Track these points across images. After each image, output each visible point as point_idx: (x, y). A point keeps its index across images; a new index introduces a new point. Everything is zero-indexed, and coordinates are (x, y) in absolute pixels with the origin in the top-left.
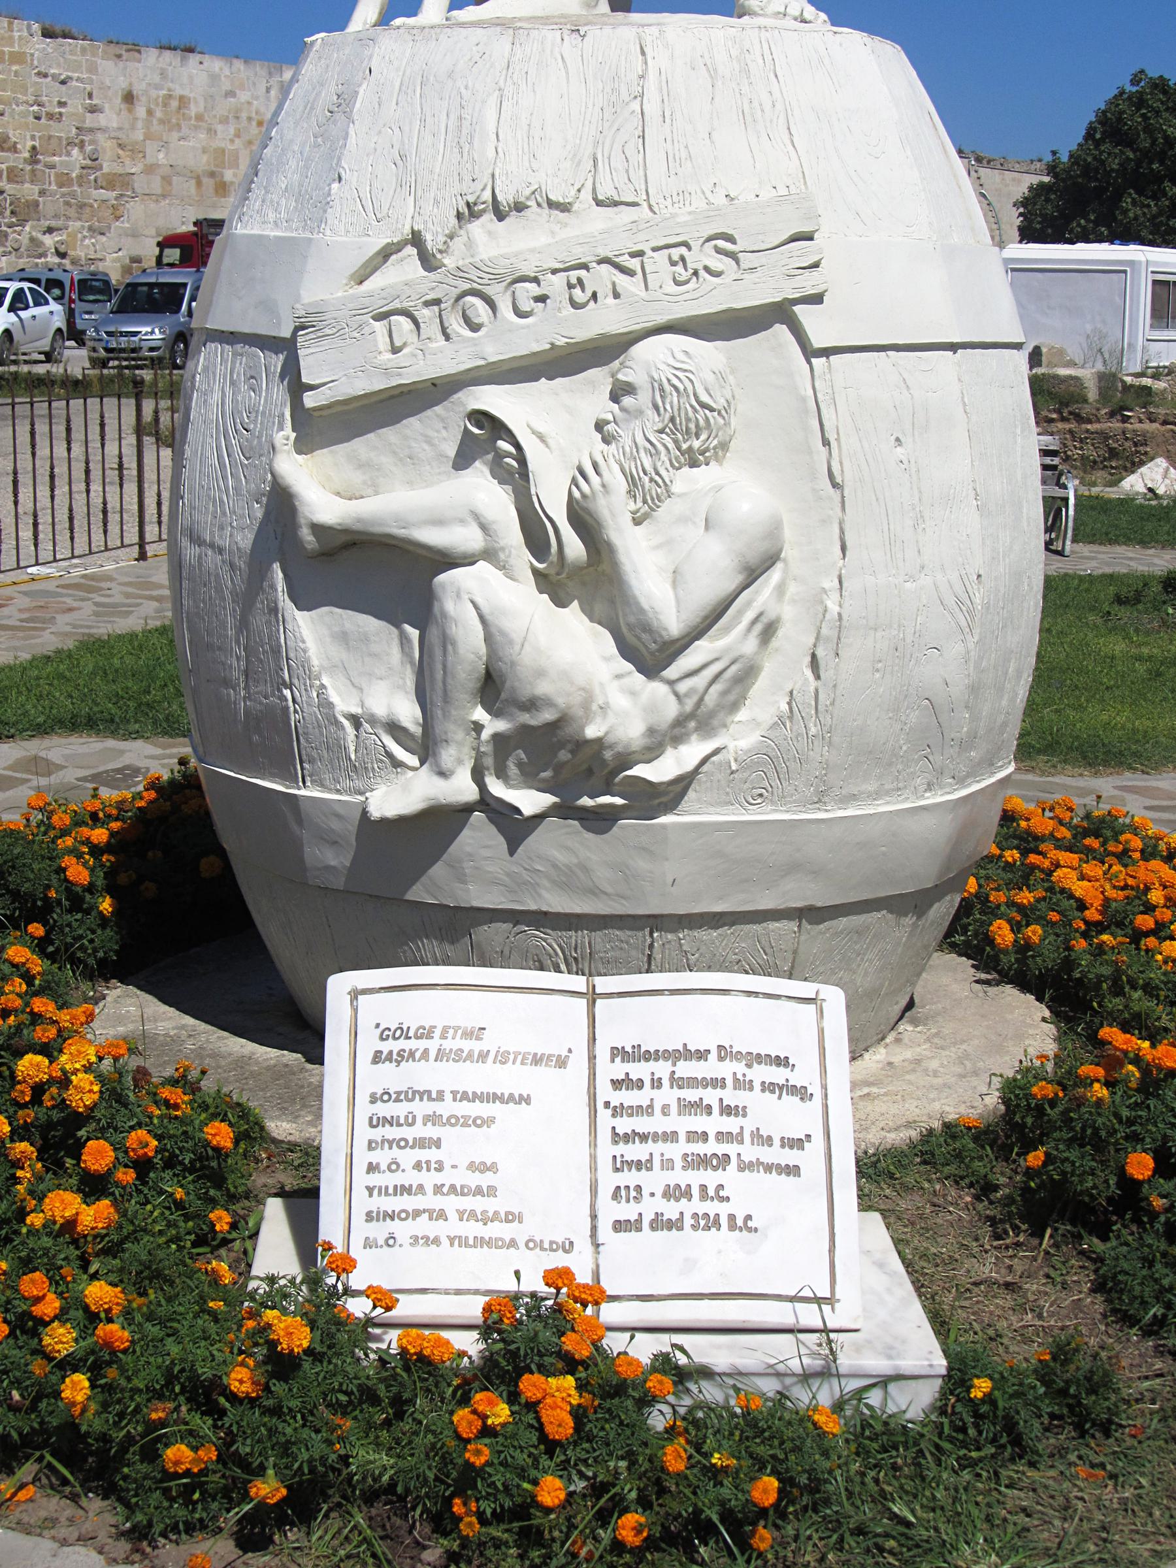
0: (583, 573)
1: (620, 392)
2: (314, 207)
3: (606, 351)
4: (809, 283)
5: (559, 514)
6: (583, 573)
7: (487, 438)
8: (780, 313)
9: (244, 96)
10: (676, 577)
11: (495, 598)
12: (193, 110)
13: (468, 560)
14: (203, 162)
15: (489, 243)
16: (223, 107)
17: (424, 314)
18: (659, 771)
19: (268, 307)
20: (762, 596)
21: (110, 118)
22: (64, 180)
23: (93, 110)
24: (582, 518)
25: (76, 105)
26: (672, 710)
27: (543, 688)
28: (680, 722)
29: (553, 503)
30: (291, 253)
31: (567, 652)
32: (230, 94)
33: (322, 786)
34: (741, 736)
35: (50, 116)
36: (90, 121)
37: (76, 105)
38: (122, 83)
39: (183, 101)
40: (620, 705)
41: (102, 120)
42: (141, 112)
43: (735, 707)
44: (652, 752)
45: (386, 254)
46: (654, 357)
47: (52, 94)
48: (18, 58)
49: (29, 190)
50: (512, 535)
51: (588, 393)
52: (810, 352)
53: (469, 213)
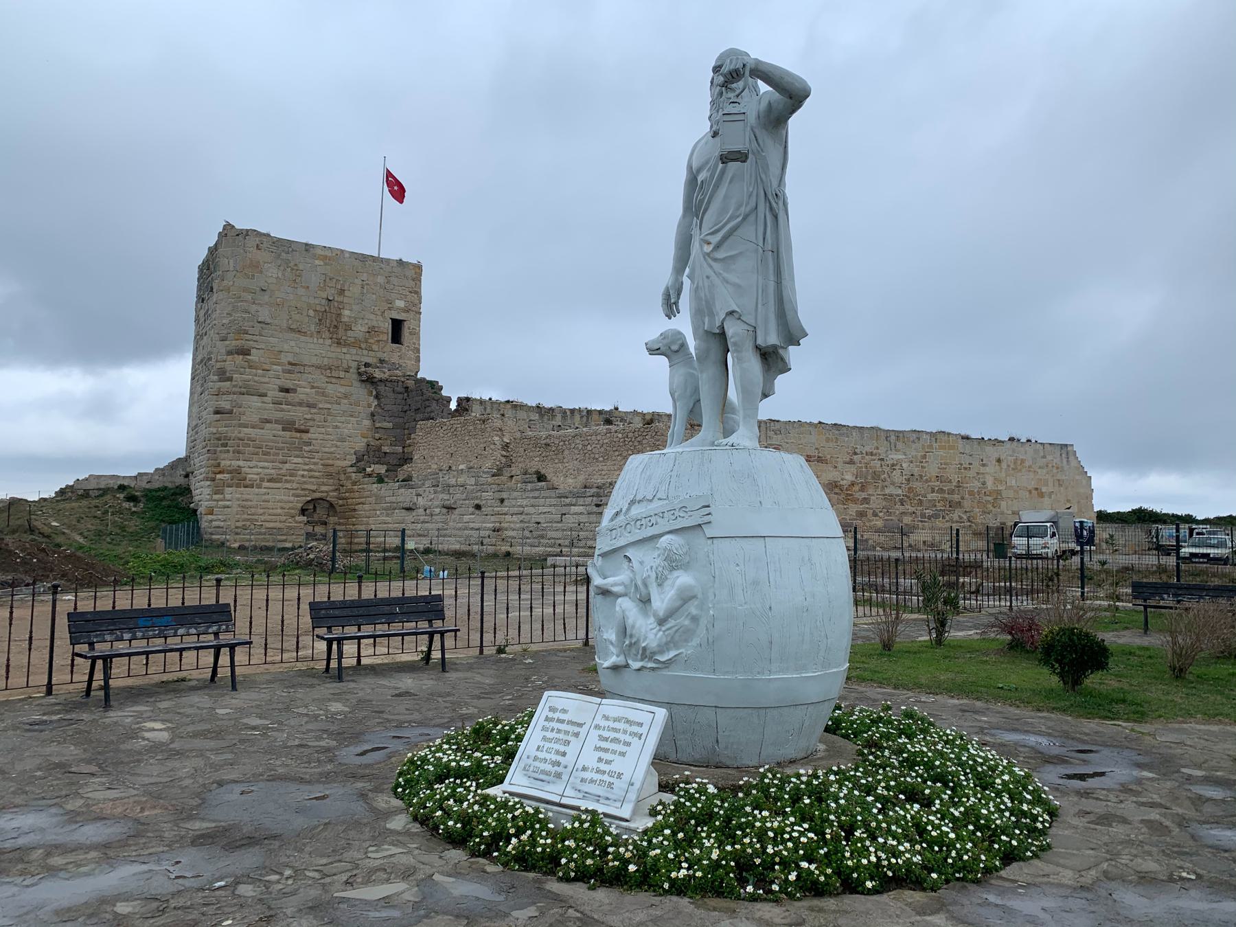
4: (706, 519)
9: (1049, 458)
12: (1027, 464)
14: (1033, 485)
15: (636, 511)
16: (1042, 462)
20: (693, 609)
21: (991, 469)
22: (971, 493)
23: (984, 465)
25: (976, 464)
28: (667, 644)
32: (1044, 457)
36: (982, 470)
37: (976, 464)
38: (996, 455)
39: (1023, 461)
41: (987, 469)
42: (1004, 465)
44: (661, 652)
47: (966, 460)
49: (956, 497)
53: (632, 502)
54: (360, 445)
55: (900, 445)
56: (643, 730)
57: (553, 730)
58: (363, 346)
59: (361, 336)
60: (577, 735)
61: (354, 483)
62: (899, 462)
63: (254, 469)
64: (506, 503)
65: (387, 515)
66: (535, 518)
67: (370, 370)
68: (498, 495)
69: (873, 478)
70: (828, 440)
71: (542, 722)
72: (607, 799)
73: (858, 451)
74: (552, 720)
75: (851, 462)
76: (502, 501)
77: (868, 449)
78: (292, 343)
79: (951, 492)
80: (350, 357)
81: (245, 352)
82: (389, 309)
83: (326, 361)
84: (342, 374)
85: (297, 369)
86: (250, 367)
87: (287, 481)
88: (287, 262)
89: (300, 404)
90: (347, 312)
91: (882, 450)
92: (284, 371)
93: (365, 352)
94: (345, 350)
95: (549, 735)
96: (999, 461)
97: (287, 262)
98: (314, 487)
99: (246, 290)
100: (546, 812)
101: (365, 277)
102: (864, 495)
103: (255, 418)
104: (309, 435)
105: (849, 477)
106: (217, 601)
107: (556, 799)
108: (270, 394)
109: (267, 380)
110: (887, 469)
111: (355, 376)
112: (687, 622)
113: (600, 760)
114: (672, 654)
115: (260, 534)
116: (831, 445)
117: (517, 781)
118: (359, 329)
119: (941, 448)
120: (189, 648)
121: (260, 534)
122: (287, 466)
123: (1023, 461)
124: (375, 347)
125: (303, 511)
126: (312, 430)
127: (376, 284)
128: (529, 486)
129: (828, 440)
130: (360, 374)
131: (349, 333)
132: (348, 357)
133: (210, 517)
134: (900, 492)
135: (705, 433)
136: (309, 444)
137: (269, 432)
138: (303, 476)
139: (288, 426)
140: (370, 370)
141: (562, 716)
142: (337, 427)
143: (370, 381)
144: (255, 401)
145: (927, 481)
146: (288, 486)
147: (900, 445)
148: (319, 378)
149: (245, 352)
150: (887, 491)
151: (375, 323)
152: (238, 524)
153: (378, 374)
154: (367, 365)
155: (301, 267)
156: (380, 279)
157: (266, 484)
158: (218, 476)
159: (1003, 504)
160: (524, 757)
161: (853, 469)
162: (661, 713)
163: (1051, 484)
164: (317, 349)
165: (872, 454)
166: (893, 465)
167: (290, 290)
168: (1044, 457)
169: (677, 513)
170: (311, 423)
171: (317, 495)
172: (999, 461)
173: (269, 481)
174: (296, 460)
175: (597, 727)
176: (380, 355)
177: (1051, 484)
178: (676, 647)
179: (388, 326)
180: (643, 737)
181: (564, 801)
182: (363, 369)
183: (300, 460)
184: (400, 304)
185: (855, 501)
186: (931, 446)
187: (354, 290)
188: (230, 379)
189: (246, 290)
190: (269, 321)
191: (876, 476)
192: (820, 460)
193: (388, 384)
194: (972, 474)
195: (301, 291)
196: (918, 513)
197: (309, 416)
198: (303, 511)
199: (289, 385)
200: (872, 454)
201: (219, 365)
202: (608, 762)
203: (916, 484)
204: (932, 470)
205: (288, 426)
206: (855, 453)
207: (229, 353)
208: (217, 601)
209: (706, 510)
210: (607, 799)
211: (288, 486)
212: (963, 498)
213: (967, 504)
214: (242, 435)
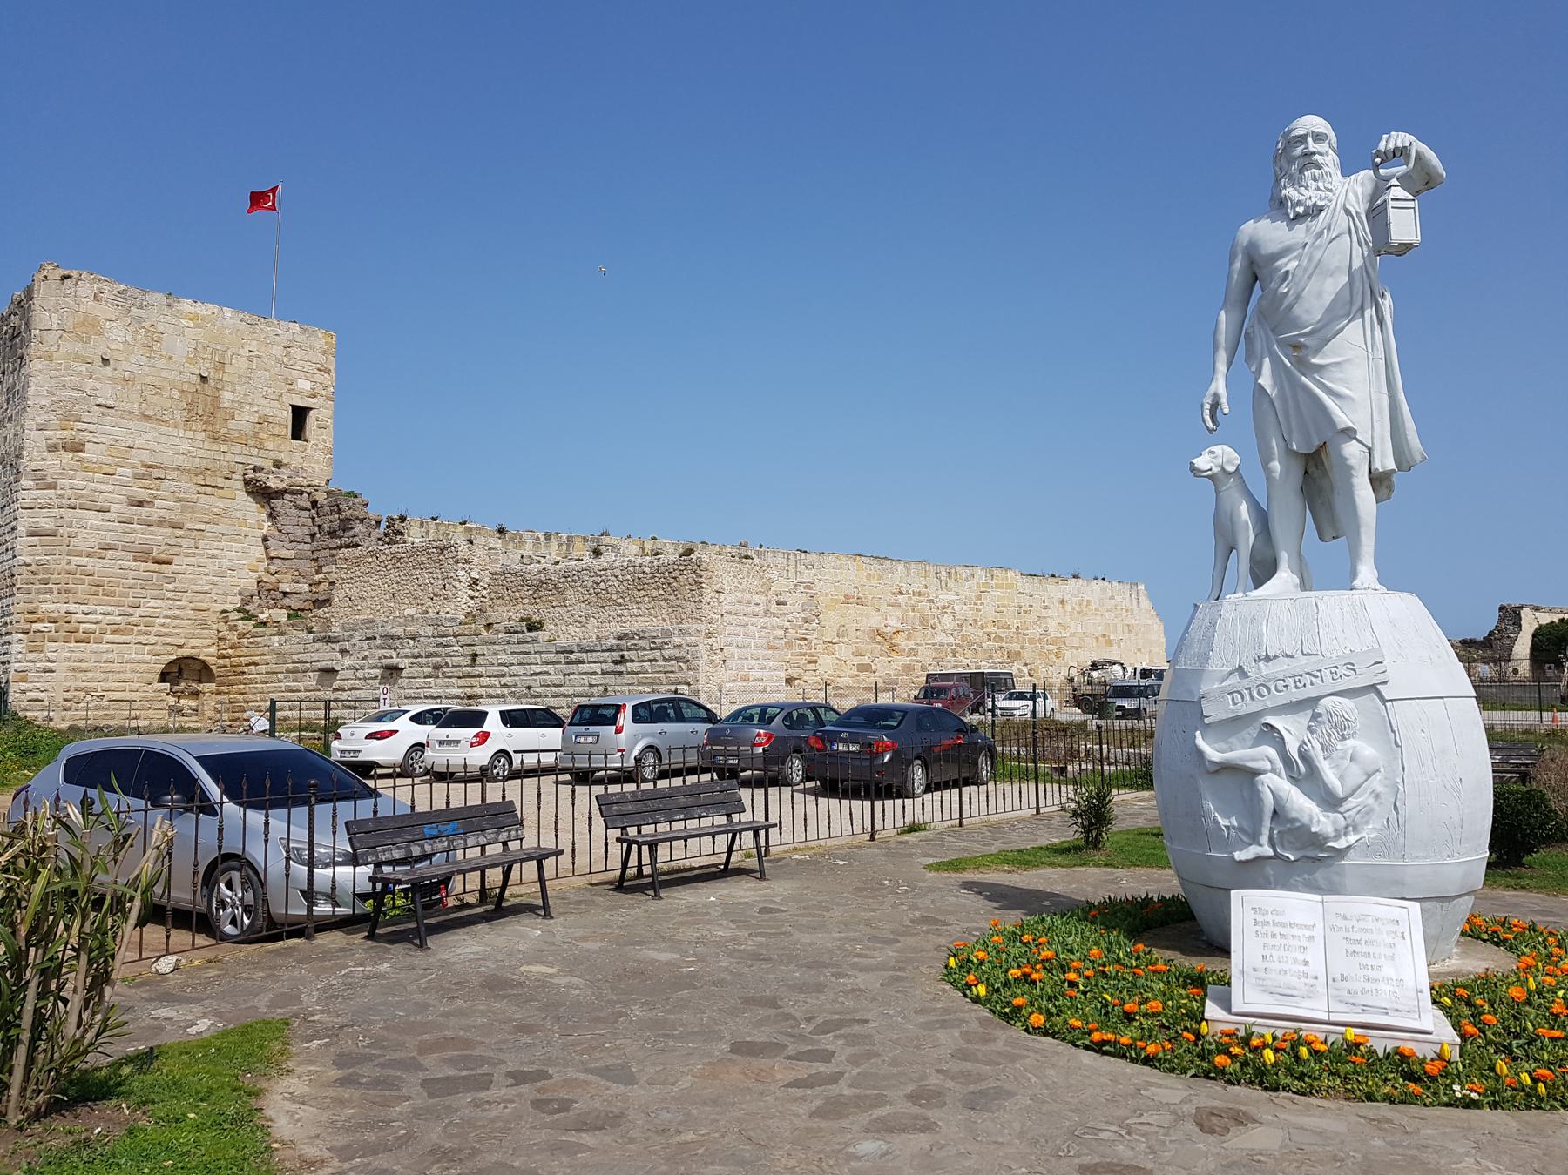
0: (1306, 774)
1: (1315, 716)
2: (1204, 658)
3: (1313, 702)
4: (1382, 678)
5: (1296, 756)
6: (1306, 774)
7: (1270, 734)
8: (1373, 688)
9: (1118, 598)
10: (1341, 778)
11: (1275, 784)
13: (1264, 772)
17: (1246, 693)
18: (1341, 844)
19: (1191, 692)
22: (1032, 641)
23: (1046, 608)
24: (1304, 756)
25: (1037, 606)
26: (1343, 823)
27: (1294, 815)
29: (1293, 750)
30: (1198, 674)
31: (1301, 804)
32: (1112, 597)
33: (1217, 850)
34: (1368, 833)
39: (1089, 602)
40: (1321, 821)
42: (1068, 607)
43: (1367, 823)
45: (1231, 673)
46: (1327, 702)
48: (1010, 586)
49: (1015, 647)
50: (1279, 765)
51: (1304, 718)
52: (1384, 701)
54: (248, 582)
55: (951, 583)
57: (1273, 936)
58: (251, 442)
59: (248, 429)
61: (242, 636)
62: (950, 604)
63: (95, 613)
64: (479, 660)
65: (295, 680)
66: (528, 680)
67: (260, 476)
68: (469, 650)
70: (869, 577)
71: (1250, 929)
74: (1264, 923)
75: (896, 604)
76: (474, 656)
78: (148, 436)
80: (238, 457)
81: (78, 448)
82: (289, 391)
83: (197, 463)
84: (220, 482)
85: (156, 473)
86: (86, 469)
87: (140, 633)
88: (139, 320)
89: (160, 524)
90: (228, 395)
91: (932, 589)
92: (136, 476)
93: (255, 452)
94: (224, 448)
95: (1270, 941)
96: (1062, 602)
97: (139, 320)
98: (181, 642)
99: (77, 357)
100: (1308, 1031)
101: (254, 346)
102: (911, 644)
103: (92, 541)
104: (173, 567)
105: (894, 623)
106: (483, 799)
107: (1324, 1017)
108: (114, 507)
109: (110, 488)
111: (241, 485)
112: (1371, 801)
113: (1362, 966)
114: (1352, 838)
115: (101, 708)
116: (873, 582)
118: (245, 420)
120: (492, 866)
121: (101, 708)
122: (139, 611)
123: (1089, 602)
124: (269, 445)
125: (163, 677)
126: (176, 560)
127: (270, 356)
128: (515, 638)
129: (869, 577)
130: (247, 483)
131: (231, 424)
132: (228, 457)
133: (23, 686)
134: (952, 640)
135: (1285, 578)
136: (172, 580)
137: (110, 565)
139: (142, 554)
140: (260, 476)
141: (1278, 919)
142: (213, 556)
143: (262, 493)
144: (92, 519)
145: (982, 627)
146: (142, 639)
148: (187, 487)
149: (78, 448)
150: (938, 639)
151: (267, 411)
152: (67, 695)
153: (273, 483)
154: (255, 469)
155: (160, 328)
156: (277, 350)
158: (36, 626)
159: (1068, 654)
163: (1119, 629)
164: (179, 445)
165: (919, 594)
167: (143, 360)
168: (1112, 597)
170: (175, 550)
172: (1062, 602)
174: (153, 603)
175: (1333, 928)
176: (275, 455)
177: (1119, 629)
178: (1356, 830)
180: (1407, 935)
181: (1334, 1018)
182: (251, 475)
183: (159, 603)
184: (305, 385)
185: (900, 653)
187: (240, 365)
188: (53, 486)
189: (77, 357)
190: (110, 403)
191: (924, 620)
192: (860, 601)
193: (287, 497)
194: (1033, 617)
195: (161, 363)
197: (173, 541)
198: (163, 677)
199: (143, 495)
200: (919, 594)
201: (34, 465)
202: (1362, 966)
204: (988, 613)
207: (52, 448)
208: (483, 799)
211: (142, 639)
213: (1027, 655)
214: (72, 567)
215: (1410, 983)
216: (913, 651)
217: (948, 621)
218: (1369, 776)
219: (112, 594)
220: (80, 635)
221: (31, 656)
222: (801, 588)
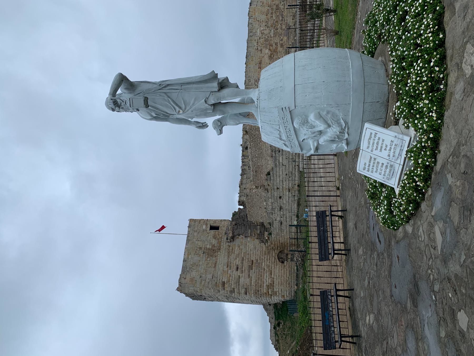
4: (287, 109)
15: (284, 138)
28: (338, 124)
35: (263, 4)
44: (341, 126)
48: (255, 10)
49: (274, 7)
54: (257, 241)
55: (254, 31)
56: (374, 132)
57: (373, 169)
58: (220, 240)
59: (216, 241)
60: (375, 159)
61: (272, 244)
63: (267, 280)
64: (279, 187)
65: (284, 231)
66: (284, 176)
67: (229, 238)
68: (276, 190)
69: (267, 41)
70: (252, 60)
71: (370, 173)
72: (401, 146)
73: (256, 48)
75: (261, 50)
76: (278, 188)
77: (256, 44)
78: (220, 266)
79: (272, 9)
80: (224, 245)
81: (224, 284)
82: (206, 231)
83: (226, 254)
84: (231, 248)
85: (229, 264)
86: (229, 281)
87: (271, 268)
88: (190, 268)
89: (242, 263)
90: (208, 246)
91: (256, 38)
92: (230, 269)
93: (222, 240)
94: (222, 247)
95: (375, 170)
97: (190, 268)
98: (274, 258)
99: (201, 283)
100: (407, 171)
101: (195, 240)
102: (274, 45)
103: (248, 280)
104: (254, 260)
105: (267, 51)
106: (319, 295)
107: (401, 167)
109: (234, 276)
110: (264, 36)
111: (231, 243)
112: (329, 116)
113: (385, 149)
114: (342, 121)
115: (291, 278)
117: (393, 183)
118: (214, 242)
119: (255, 14)
120: (337, 306)
121: (291, 278)
122: (266, 268)
124: (221, 236)
125: (283, 262)
126: (252, 259)
127: (197, 236)
128: (272, 178)
129: (252, 60)
130: (231, 242)
131: (216, 245)
132: (224, 246)
133: (285, 296)
134: (273, 30)
136: (257, 260)
137: (253, 276)
138: (269, 262)
139: (250, 268)
140: (229, 238)
142: (251, 250)
143: (233, 238)
144: (242, 280)
146: (273, 268)
147: (254, 31)
148: (233, 256)
149: (224, 284)
150: (272, 36)
151: (212, 236)
152: (288, 286)
153: (231, 235)
154: (227, 239)
155: (192, 263)
156: (196, 234)
157: (273, 276)
160: (383, 180)
161: (264, 50)
162: (367, 125)
164: (222, 258)
165: (257, 42)
166: (262, 34)
167: (200, 267)
169: (285, 121)
170: (249, 259)
171: (276, 257)
173: (271, 275)
175: (372, 151)
176: (223, 234)
178: (339, 120)
179: (213, 231)
180: (376, 132)
181: (402, 163)
182: (229, 240)
183: (263, 264)
184: (204, 227)
185: (276, 48)
186: (254, 19)
187: (200, 243)
188: (234, 289)
189: (201, 283)
190: (212, 275)
191: (266, 40)
192: (260, 63)
193: (234, 231)
195: (201, 263)
196: (281, 22)
197: (247, 260)
198: (283, 262)
199: (235, 267)
201: (229, 293)
202: (386, 146)
203: (269, 24)
204: (264, 17)
205: (250, 268)
206: (258, 49)
207: (224, 289)
208: (319, 295)
209: (284, 109)
210: (401, 146)
211: (273, 268)
212: (275, 4)
214: (254, 285)
215: (393, 139)
216: (276, 44)
217: (266, 32)
218: (321, 117)
219: (261, 275)
220: (272, 283)
221: (278, 294)
222: (256, 83)
